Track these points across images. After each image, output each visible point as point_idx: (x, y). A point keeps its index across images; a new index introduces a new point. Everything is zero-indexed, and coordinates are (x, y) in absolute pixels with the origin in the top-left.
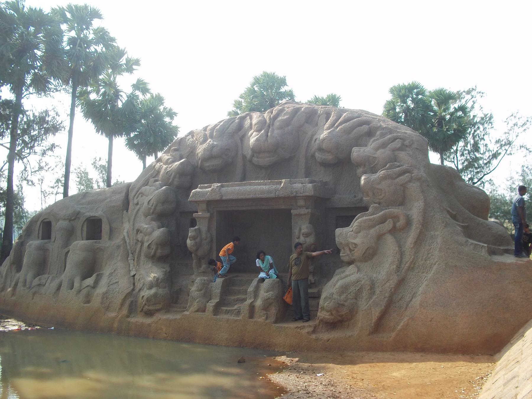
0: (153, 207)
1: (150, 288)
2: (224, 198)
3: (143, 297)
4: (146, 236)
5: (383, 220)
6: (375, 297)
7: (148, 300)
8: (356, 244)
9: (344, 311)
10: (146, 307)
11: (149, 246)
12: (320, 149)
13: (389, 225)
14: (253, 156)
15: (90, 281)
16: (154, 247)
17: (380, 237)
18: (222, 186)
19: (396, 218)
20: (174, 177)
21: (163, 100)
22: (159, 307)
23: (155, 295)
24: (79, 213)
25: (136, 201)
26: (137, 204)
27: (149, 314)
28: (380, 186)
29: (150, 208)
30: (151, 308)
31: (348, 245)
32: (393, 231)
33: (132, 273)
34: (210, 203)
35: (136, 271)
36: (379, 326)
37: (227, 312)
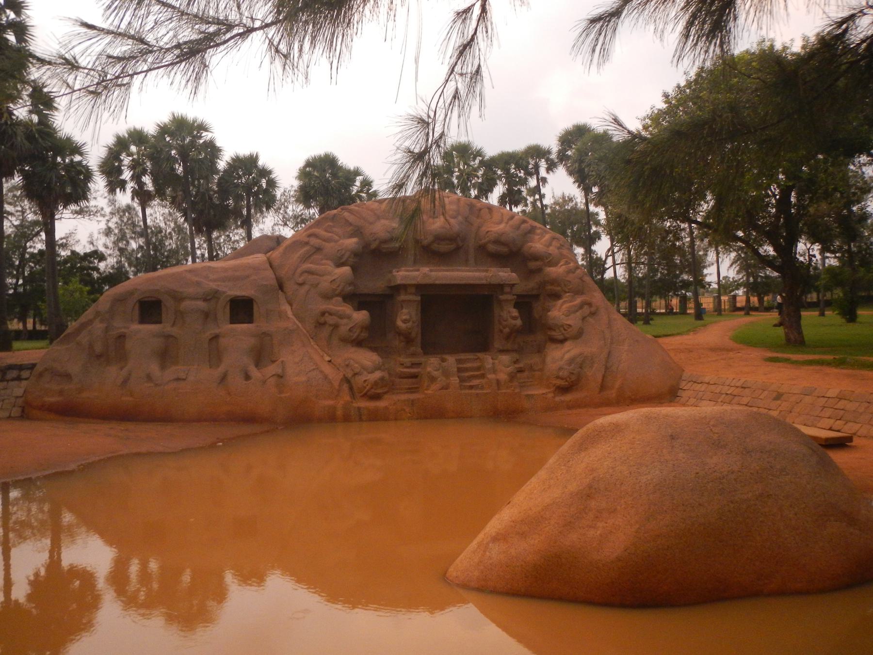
0: (340, 288)
1: (372, 372)
2: (437, 282)
3: (365, 381)
4: (342, 318)
5: (581, 307)
6: (596, 365)
7: (376, 384)
8: (570, 325)
9: (573, 378)
10: (373, 390)
11: (350, 330)
12: (497, 242)
13: (586, 310)
14: (433, 242)
15: (272, 369)
16: (358, 331)
17: (584, 319)
18: (431, 271)
19: (590, 305)
20: (349, 257)
21: (237, 157)
22: (386, 390)
23: (382, 379)
24: (217, 292)
25: (300, 280)
26: (301, 285)
27: (377, 397)
28: (568, 279)
29: (336, 290)
30: (379, 391)
31: (562, 326)
32: (592, 314)
33: (327, 358)
34: (420, 288)
35: (330, 356)
36: (603, 387)
37: (471, 387)
